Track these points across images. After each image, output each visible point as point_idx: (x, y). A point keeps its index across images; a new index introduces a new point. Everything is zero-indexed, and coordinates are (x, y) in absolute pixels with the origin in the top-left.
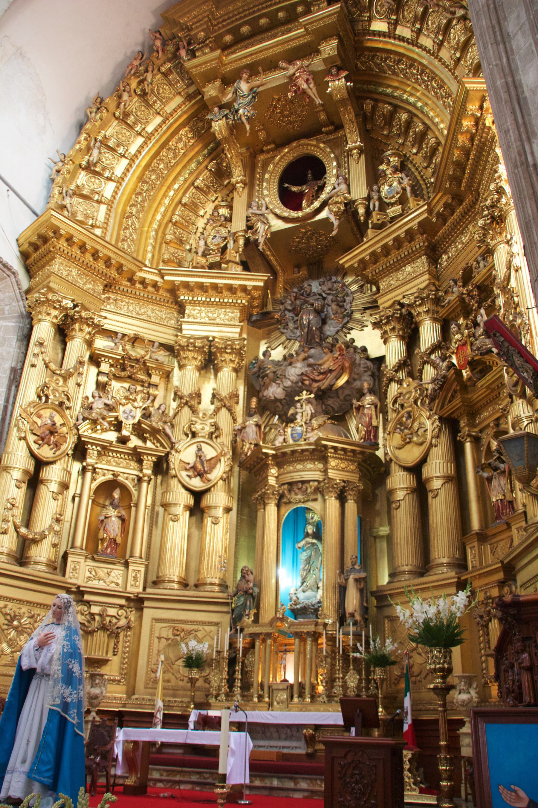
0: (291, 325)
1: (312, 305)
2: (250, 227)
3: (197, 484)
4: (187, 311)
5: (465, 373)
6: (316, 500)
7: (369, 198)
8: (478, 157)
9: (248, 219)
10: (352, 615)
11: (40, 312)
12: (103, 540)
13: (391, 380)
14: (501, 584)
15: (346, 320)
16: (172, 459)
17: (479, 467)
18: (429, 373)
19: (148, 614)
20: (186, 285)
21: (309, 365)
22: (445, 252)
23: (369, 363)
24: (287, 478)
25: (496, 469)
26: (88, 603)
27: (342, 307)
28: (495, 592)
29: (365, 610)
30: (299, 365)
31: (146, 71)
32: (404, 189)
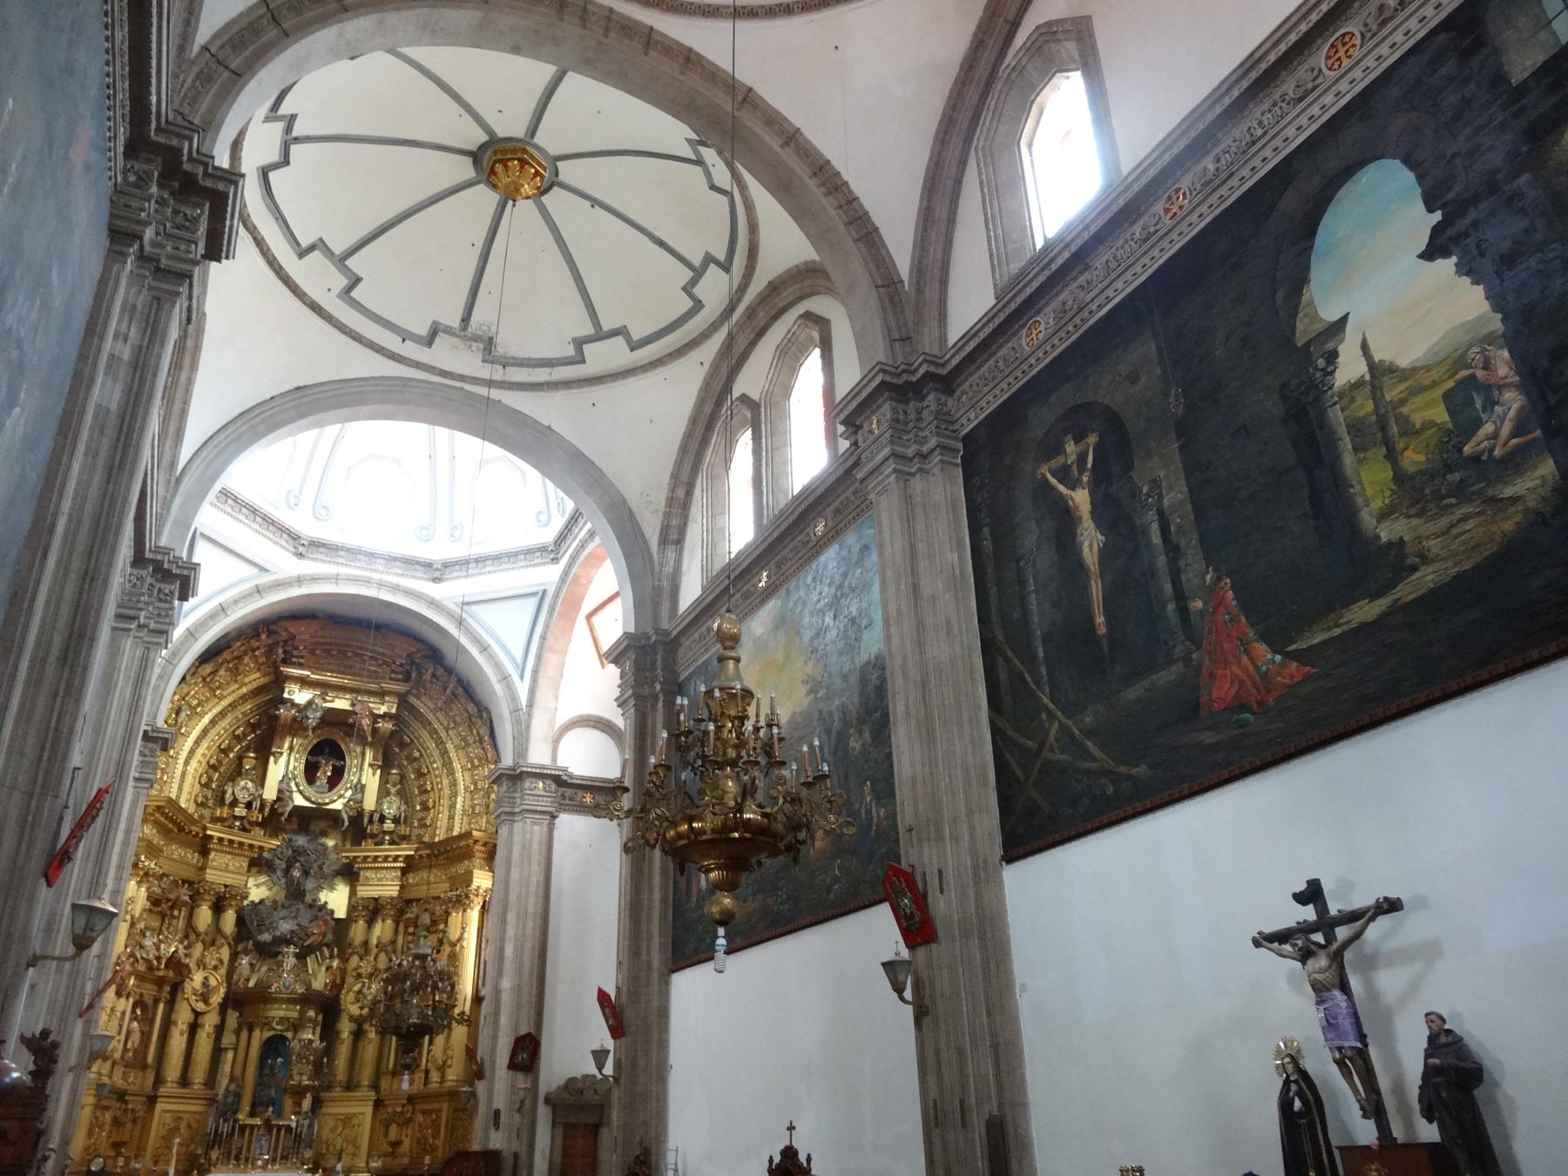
0: (279, 873)
2: (279, 799)
3: (200, 1006)
4: (211, 857)
9: (280, 791)
14: (404, 1106)
16: (186, 985)
19: (159, 1107)
20: (221, 840)
21: (298, 925)
23: (333, 923)
26: (126, 1102)
27: (321, 869)
28: (399, 1109)
30: (291, 922)
31: (245, 653)
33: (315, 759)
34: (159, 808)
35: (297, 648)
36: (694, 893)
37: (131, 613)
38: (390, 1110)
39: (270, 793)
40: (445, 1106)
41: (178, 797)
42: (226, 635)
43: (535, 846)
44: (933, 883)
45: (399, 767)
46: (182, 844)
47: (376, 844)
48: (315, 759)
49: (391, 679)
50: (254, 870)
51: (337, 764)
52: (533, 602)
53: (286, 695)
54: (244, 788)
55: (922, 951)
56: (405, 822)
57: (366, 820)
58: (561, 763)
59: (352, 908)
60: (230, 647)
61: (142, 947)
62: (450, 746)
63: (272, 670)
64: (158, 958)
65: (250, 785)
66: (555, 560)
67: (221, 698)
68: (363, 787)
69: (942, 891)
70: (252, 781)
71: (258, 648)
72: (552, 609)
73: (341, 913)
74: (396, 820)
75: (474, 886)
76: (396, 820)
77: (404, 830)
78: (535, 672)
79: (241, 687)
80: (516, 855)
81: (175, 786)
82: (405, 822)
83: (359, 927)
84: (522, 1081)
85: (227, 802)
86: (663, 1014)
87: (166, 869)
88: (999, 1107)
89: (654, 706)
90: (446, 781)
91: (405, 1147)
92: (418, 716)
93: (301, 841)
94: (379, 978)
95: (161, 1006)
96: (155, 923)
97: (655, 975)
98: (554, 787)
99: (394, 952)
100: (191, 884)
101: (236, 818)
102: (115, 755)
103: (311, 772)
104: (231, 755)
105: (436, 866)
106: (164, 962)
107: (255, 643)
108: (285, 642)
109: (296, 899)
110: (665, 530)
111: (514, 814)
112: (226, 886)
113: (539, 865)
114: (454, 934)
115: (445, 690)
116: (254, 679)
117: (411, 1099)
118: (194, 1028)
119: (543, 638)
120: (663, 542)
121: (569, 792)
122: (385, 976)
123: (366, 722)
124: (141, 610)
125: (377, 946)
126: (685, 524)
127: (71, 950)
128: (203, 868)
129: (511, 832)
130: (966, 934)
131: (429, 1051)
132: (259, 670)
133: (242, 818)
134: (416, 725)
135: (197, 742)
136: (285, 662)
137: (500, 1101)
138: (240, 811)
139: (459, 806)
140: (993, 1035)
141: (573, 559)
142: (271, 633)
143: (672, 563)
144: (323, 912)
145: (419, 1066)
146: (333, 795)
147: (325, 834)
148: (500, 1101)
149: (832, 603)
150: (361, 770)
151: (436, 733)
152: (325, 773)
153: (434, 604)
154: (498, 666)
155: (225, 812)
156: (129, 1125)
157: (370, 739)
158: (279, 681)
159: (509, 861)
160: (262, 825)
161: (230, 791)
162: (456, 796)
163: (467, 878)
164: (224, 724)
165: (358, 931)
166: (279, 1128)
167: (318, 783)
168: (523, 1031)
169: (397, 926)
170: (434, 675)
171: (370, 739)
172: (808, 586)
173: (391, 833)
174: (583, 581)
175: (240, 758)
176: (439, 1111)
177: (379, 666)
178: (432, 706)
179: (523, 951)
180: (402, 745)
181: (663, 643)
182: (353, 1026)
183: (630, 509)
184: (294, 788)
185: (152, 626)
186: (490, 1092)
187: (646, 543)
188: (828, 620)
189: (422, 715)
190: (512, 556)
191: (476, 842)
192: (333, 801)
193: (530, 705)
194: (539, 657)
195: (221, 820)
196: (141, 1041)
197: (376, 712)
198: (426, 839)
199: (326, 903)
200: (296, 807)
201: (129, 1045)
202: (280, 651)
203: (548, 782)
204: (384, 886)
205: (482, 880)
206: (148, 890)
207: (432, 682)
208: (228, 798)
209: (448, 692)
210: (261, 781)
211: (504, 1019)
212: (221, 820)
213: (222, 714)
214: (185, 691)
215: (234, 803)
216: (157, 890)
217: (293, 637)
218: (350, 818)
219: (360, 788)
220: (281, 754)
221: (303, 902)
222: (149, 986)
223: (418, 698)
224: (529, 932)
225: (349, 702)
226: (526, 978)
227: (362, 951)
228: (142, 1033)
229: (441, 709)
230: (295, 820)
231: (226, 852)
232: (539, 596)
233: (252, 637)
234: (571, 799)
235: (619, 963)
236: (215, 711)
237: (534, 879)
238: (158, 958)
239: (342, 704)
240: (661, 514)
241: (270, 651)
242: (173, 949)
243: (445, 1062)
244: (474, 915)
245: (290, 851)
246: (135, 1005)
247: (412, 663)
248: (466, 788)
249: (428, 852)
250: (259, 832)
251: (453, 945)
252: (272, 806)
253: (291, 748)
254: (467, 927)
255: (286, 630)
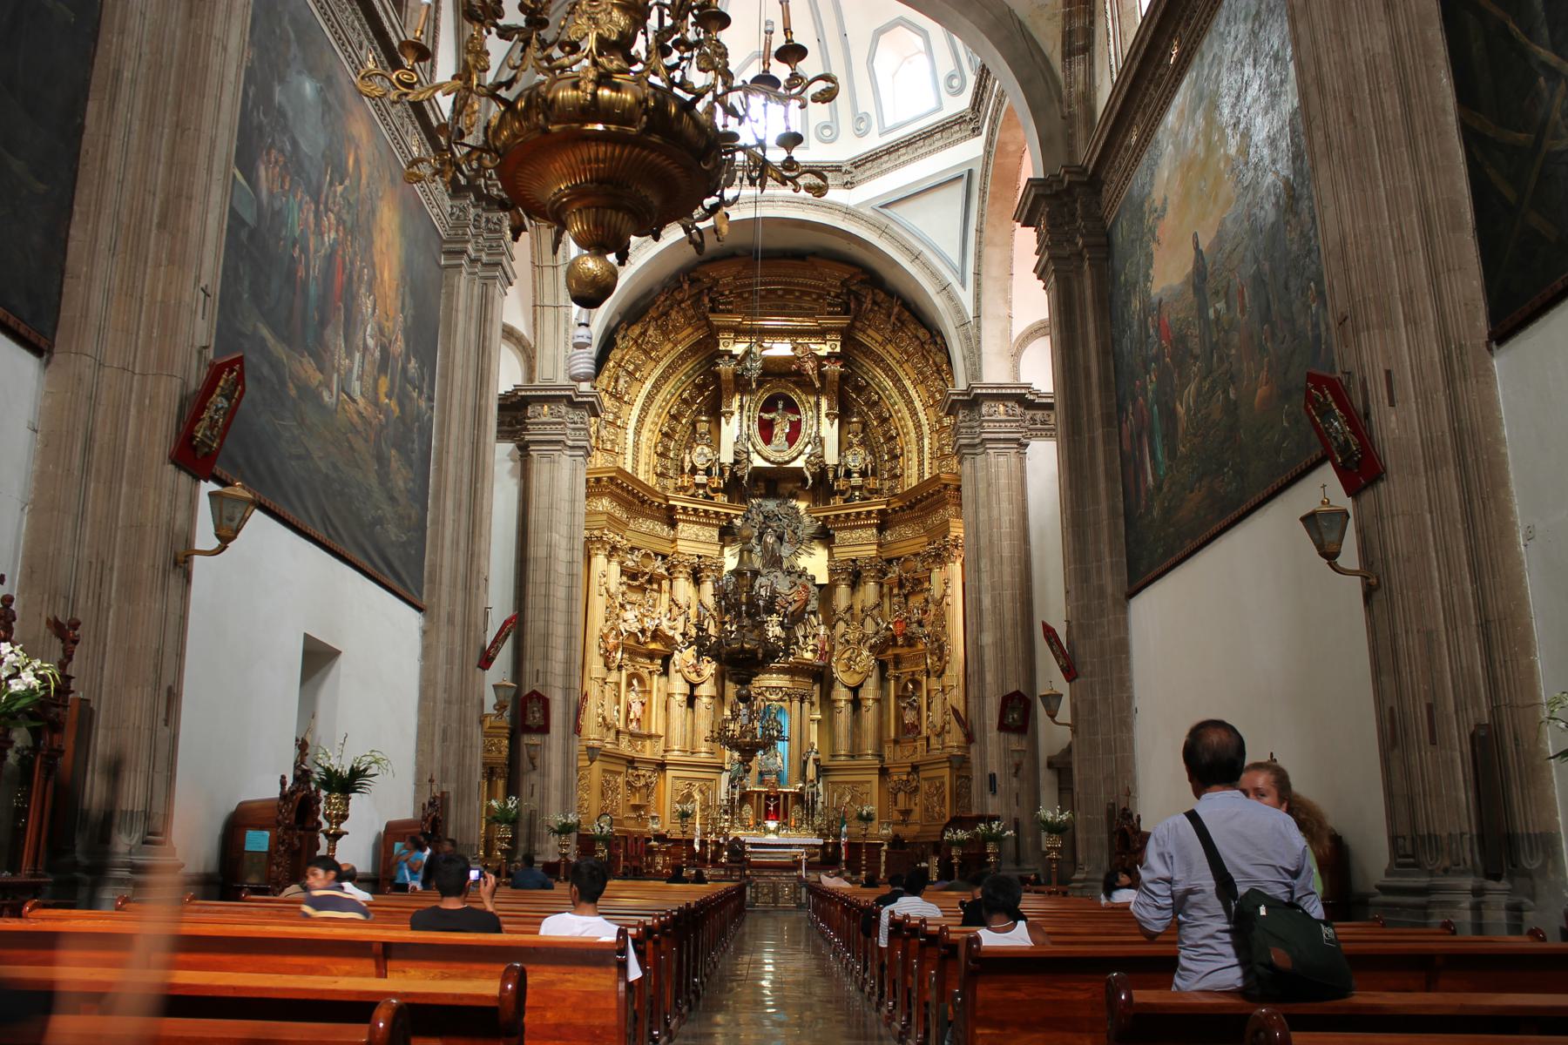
1: (776, 531)
2: (736, 462)
3: (693, 677)
5: (900, 641)
6: (785, 701)
7: (837, 466)
8: (932, 505)
9: (736, 453)
10: (812, 781)
11: (598, 549)
12: (631, 720)
13: (840, 619)
14: (909, 774)
15: (798, 546)
17: (897, 697)
18: (870, 627)
19: (670, 773)
20: (684, 508)
22: (889, 528)
23: (816, 590)
24: (767, 683)
25: (911, 705)
27: (796, 534)
28: (905, 777)
29: (818, 778)
31: (671, 307)
32: (866, 466)
33: (772, 416)
34: (611, 479)
35: (722, 295)
36: (1143, 494)
37: (458, 246)
38: (895, 778)
39: (727, 457)
40: (946, 772)
41: (635, 469)
42: (650, 291)
43: (1003, 481)
44: (1379, 390)
45: (859, 414)
46: (648, 517)
47: (845, 501)
48: (766, 416)
49: (829, 313)
50: (728, 539)
51: (792, 419)
52: (960, 188)
53: (722, 348)
54: (700, 454)
55: (1368, 497)
56: (874, 473)
57: (831, 475)
58: (1024, 379)
59: (832, 572)
60: (653, 302)
61: (625, 621)
62: (907, 383)
63: (703, 322)
64: (643, 631)
65: (706, 450)
66: (976, 131)
67: (657, 361)
68: (822, 441)
69: (1392, 404)
70: (708, 446)
71: (682, 301)
72: (983, 191)
73: (823, 579)
74: (863, 474)
75: (951, 537)
76: (863, 474)
77: (873, 483)
78: (978, 274)
79: (675, 345)
80: (982, 493)
81: (629, 457)
82: (874, 473)
83: (843, 591)
84: (1015, 742)
85: (687, 471)
86: (1122, 648)
87: (635, 543)
88: (1491, 713)
89: (1079, 271)
90: (910, 424)
91: (916, 815)
92: (868, 352)
93: (771, 505)
94: (868, 644)
95: (655, 677)
96: (634, 597)
97: (1110, 602)
98: (1018, 410)
99: (881, 615)
100: (664, 557)
101: (698, 486)
102: (470, 402)
103: (766, 430)
104: (684, 421)
105: (912, 519)
106: (649, 634)
107: (679, 296)
108: (710, 289)
109: (773, 566)
110: (1068, 36)
111: (974, 446)
112: (699, 557)
113: (1011, 503)
114: (936, 592)
115: (889, 317)
116: (688, 337)
117: (915, 768)
118: (691, 700)
119: (979, 231)
120: (1068, 53)
121: (1039, 415)
122: (873, 641)
123: (809, 366)
124: (468, 241)
125: (862, 611)
126: (1092, 23)
127: (215, 543)
128: (674, 541)
129: (974, 467)
130: (1433, 464)
131: (928, 716)
132: (690, 324)
133: (703, 486)
134: (868, 364)
135: (645, 410)
136: (713, 310)
137: (994, 766)
138: (701, 478)
139: (926, 449)
140: (1481, 607)
141: (994, 121)
142: (693, 281)
143: (1081, 78)
144: (804, 578)
145: (920, 733)
146: (793, 451)
147: (795, 496)
148: (994, 766)
149: (1250, 43)
150: (818, 423)
151: (891, 369)
152: (783, 430)
153: (849, 213)
154: (934, 275)
155: (686, 481)
156: (644, 791)
157: (818, 385)
158: (713, 334)
159: (976, 501)
160: (726, 490)
161: (687, 458)
162: (922, 439)
163: (944, 529)
164: (667, 389)
165: (842, 595)
166: (786, 794)
167: (775, 441)
168: (1012, 688)
169: (881, 586)
170: (875, 303)
171: (818, 385)
172: (1222, 34)
173: (860, 488)
174: (1012, 148)
175: (694, 424)
176: (943, 777)
177: (815, 300)
178: (880, 339)
179: (1001, 602)
180: (860, 390)
181: (1082, 184)
182: (850, 696)
183: (1020, 22)
184: (751, 449)
185: (485, 258)
186: (983, 754)
187: (1046, 61)
188: (1248, 70)
189: (873, 352)
190: (926, 135)
191: (946, 486)
192: (794, 459)
193: (978, 316)
194: (979, 256)
195: (683, 489)
196: (644, 712)
197: (819, 353)
198: (899, 491)
199: (805, 568)
200: (754, 468)
201: (632, 716)
202: (706, 300)
203: (1010, 404)
204: (861, 544)
205: (957, 530)
206: (621, 563)
207: (871, 310)
208: (687, 467)
209: (893, 319)
210: (715, 445)
211: (989, 678)
212: (683, 489)
213: (664, 377)
214: (619, 356)
215: (694, 470)
216: (630, 564)
217: (716, 282)
218: (813, 475)
219: (819, 441)
220: (732, 413)
221: (781, 568)
222: (639, 659)
223: (864, 332)
224: (1007, 578)
225: (790, 347)
226: (1009, 631)
227: (848, 616)
228: (643, 704)
229: (890, 341)
230: (761, 484)
231: (694, 522)
232: (966, 176)
233: (675, 289)
234: (1043, 423)
235: (1067, 592)
236: (657, 372)
237: (1006, 519)
238: (643, 631)
239: (781, 349)
240: (1059, 18)
241: (697, 303)
242: (657, 621)
243: (943, 727)
244: (955, 569)
245: (761, 517)
246: (631, 677)
247: (850, 292)
248: (931, 427)
249: (901, 504)
250: (721, 498)
251: (939, 603)
252: (731, 470)
253: (741, 407)
254: (951, 580)
255: (708, 276)
